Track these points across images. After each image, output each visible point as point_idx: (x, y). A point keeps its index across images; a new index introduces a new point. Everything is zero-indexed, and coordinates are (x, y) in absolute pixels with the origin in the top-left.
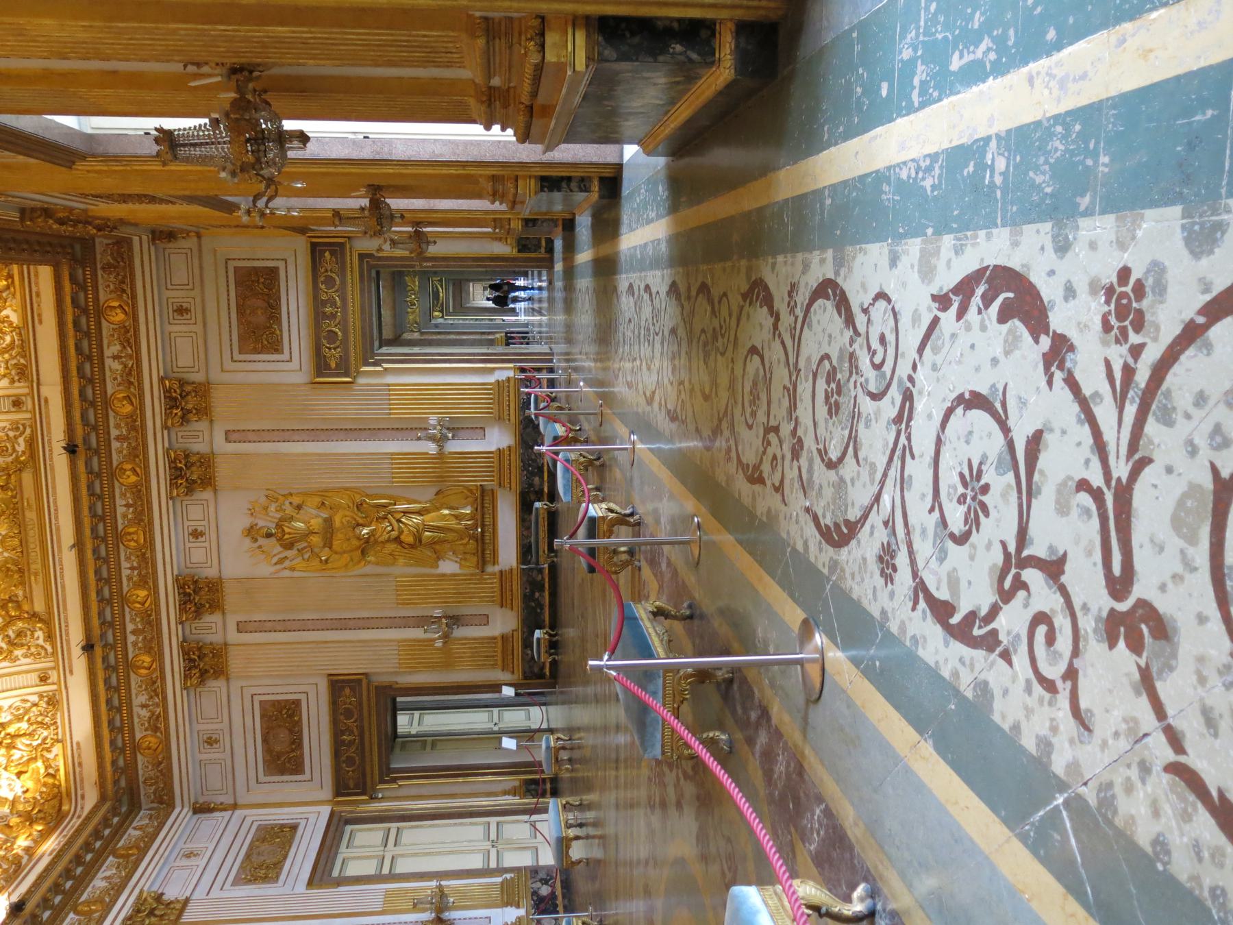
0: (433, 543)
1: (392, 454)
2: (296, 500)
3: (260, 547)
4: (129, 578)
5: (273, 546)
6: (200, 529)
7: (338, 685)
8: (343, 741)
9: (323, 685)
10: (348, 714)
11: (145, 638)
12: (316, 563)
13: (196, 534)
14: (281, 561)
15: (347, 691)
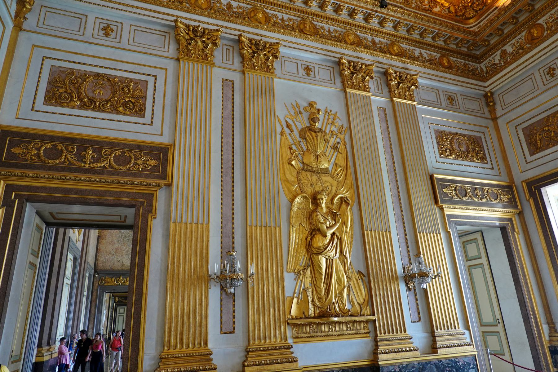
0: (313, 265)
1: (390, 232)
2: (341, 147)
3: (301, 113)
4: (276, 16)
5: (303, 122)
6: (312, 73)
7: (162, 154)
8: (86, 149)
9: (164, 140)
10: (123, 160)
11: (224, 10)
12: (287, 154)
13: (308, 70)
14: (288, 126)
15: (153, 162)
